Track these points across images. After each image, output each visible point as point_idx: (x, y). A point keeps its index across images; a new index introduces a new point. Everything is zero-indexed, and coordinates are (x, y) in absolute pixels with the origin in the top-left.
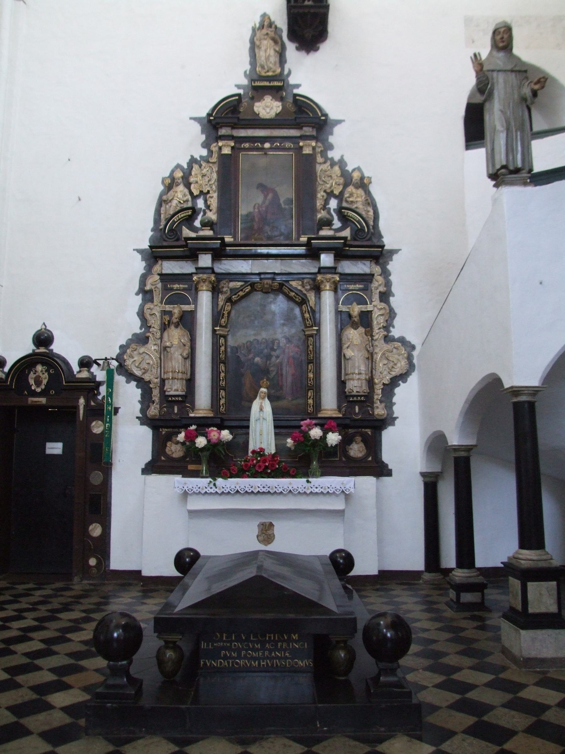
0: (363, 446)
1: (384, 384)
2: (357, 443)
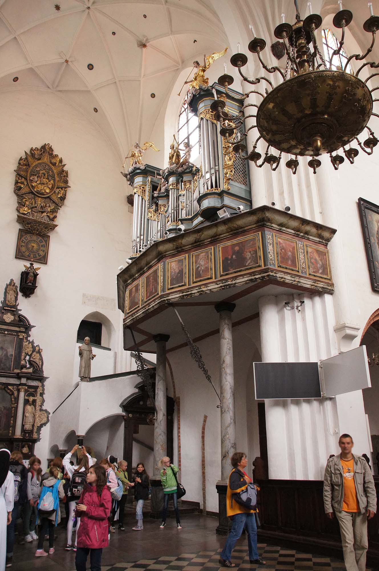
0: (28, 449)
1: (38, 426)
2: (26, 448)
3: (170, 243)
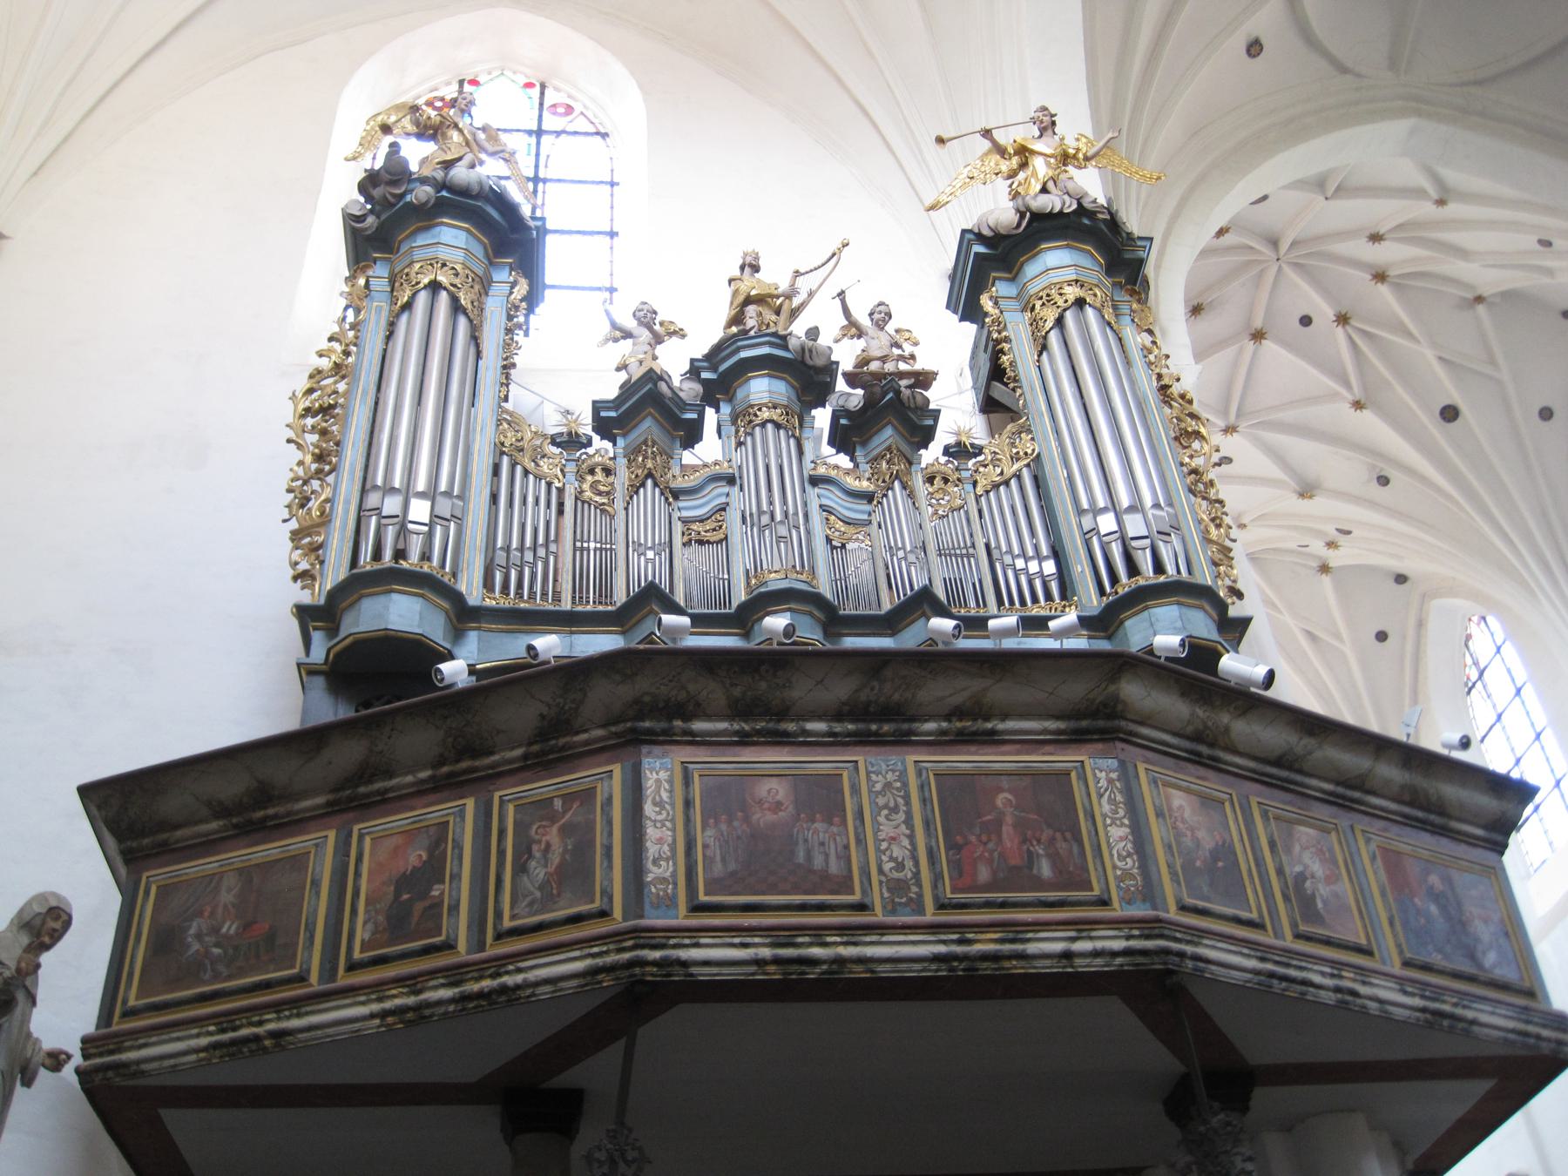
3: (1183, 695)
